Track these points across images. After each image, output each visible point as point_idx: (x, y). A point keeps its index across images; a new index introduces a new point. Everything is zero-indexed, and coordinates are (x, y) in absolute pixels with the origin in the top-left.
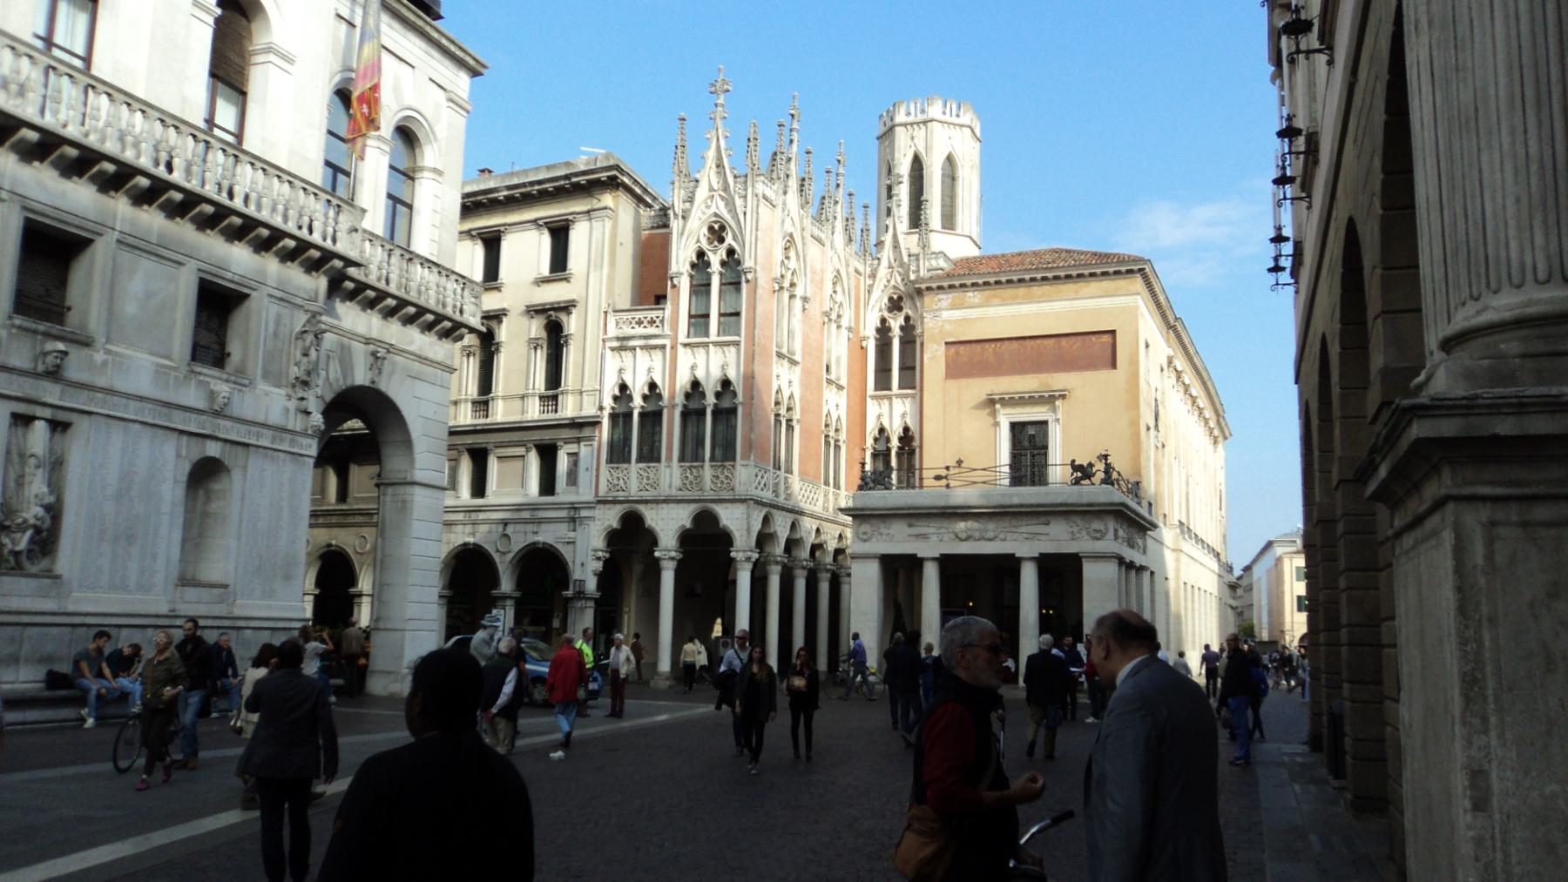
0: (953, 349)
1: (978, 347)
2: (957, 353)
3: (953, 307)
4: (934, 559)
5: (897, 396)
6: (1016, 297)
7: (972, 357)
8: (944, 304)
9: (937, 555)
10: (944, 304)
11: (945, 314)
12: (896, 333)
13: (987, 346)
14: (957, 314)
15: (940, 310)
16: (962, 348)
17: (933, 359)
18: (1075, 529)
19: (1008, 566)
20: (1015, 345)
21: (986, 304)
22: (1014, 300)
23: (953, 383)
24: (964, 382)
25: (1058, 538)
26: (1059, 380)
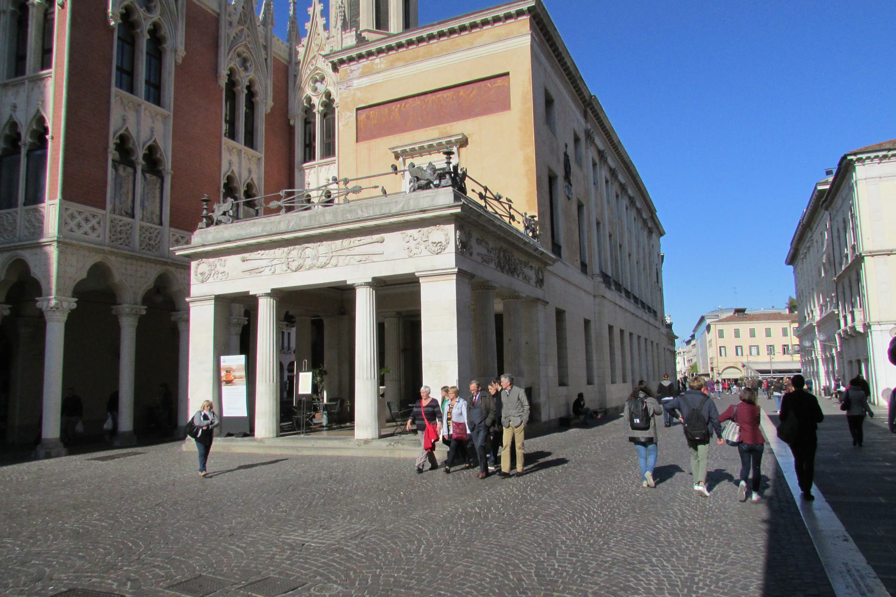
0: (363, 115)
1: (384, 109)
2: (368, 117)
3: (363, 75)
4: (267, 295)
5: (321, 165)
6: (418, 57)
7: (377, 119)
8: (356, 74)
9: (269, 291)
10: (356, 74)
11: (356, 83)
12: (318, 109)
13: (393, 106)
14: (365, 81)
15: (351, 80)
16: (372, 112)
17: (345, 125)
18: (412, 244)
19: (339, 298)
20: (418, 101)
21: (391, 66)
22: (416, 60)
23: (363, 145)
24: (373, 142)
25: (394, 256)
26: (458, 128)
